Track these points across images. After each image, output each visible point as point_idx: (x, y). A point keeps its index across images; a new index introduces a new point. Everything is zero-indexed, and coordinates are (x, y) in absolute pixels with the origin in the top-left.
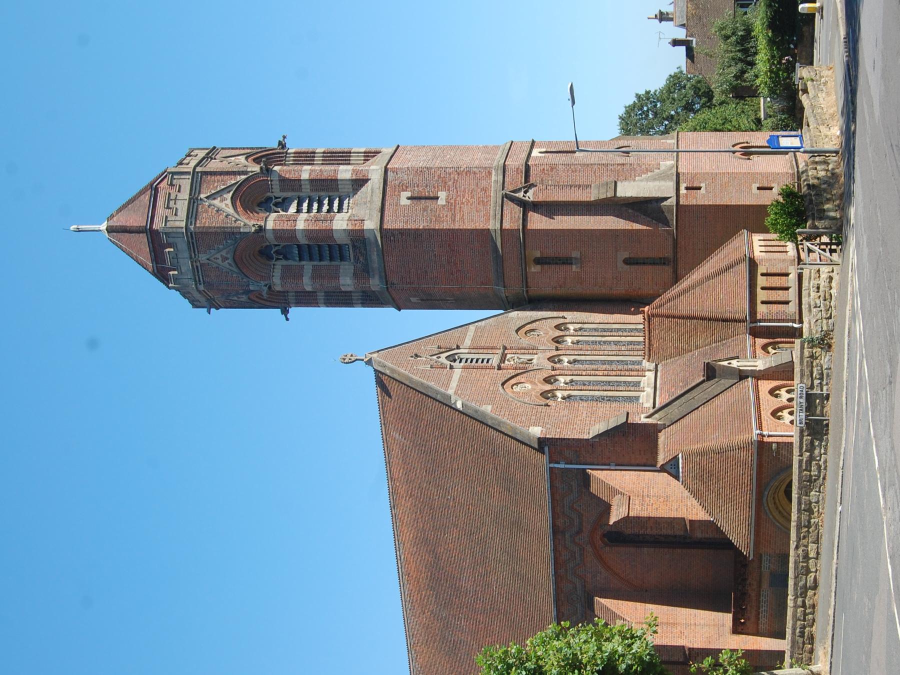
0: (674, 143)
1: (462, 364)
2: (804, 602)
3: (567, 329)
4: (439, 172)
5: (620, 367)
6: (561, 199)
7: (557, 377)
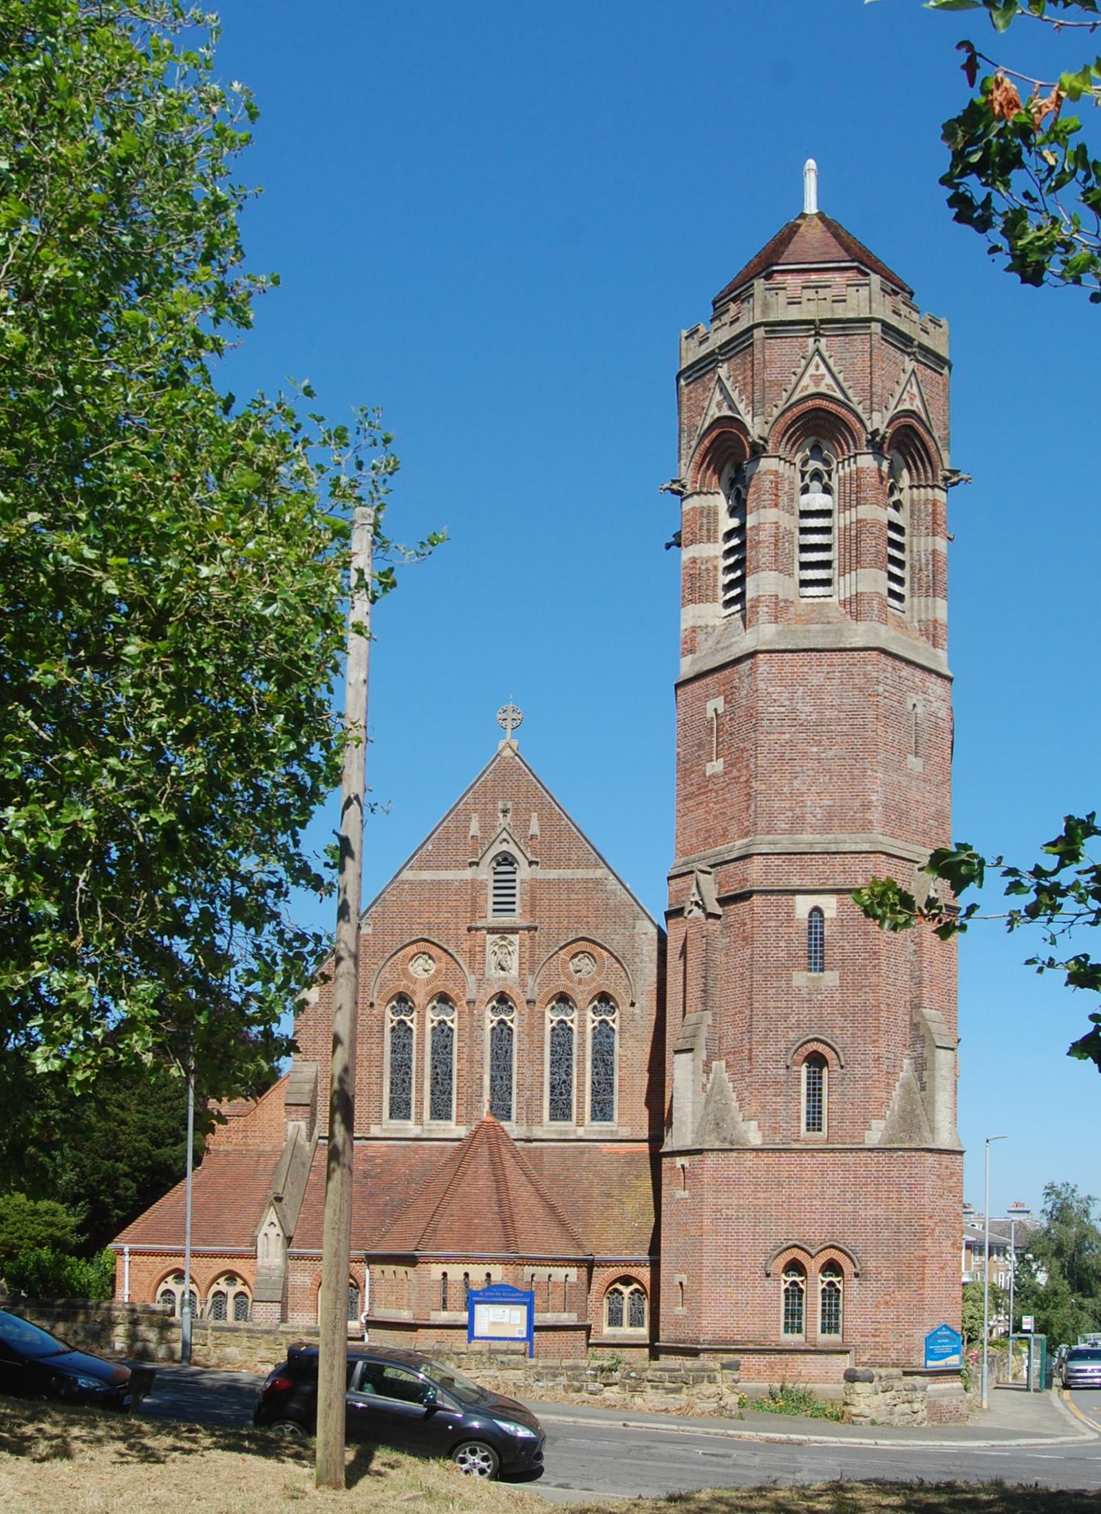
0: (863, 1143)
4: (749, 746)
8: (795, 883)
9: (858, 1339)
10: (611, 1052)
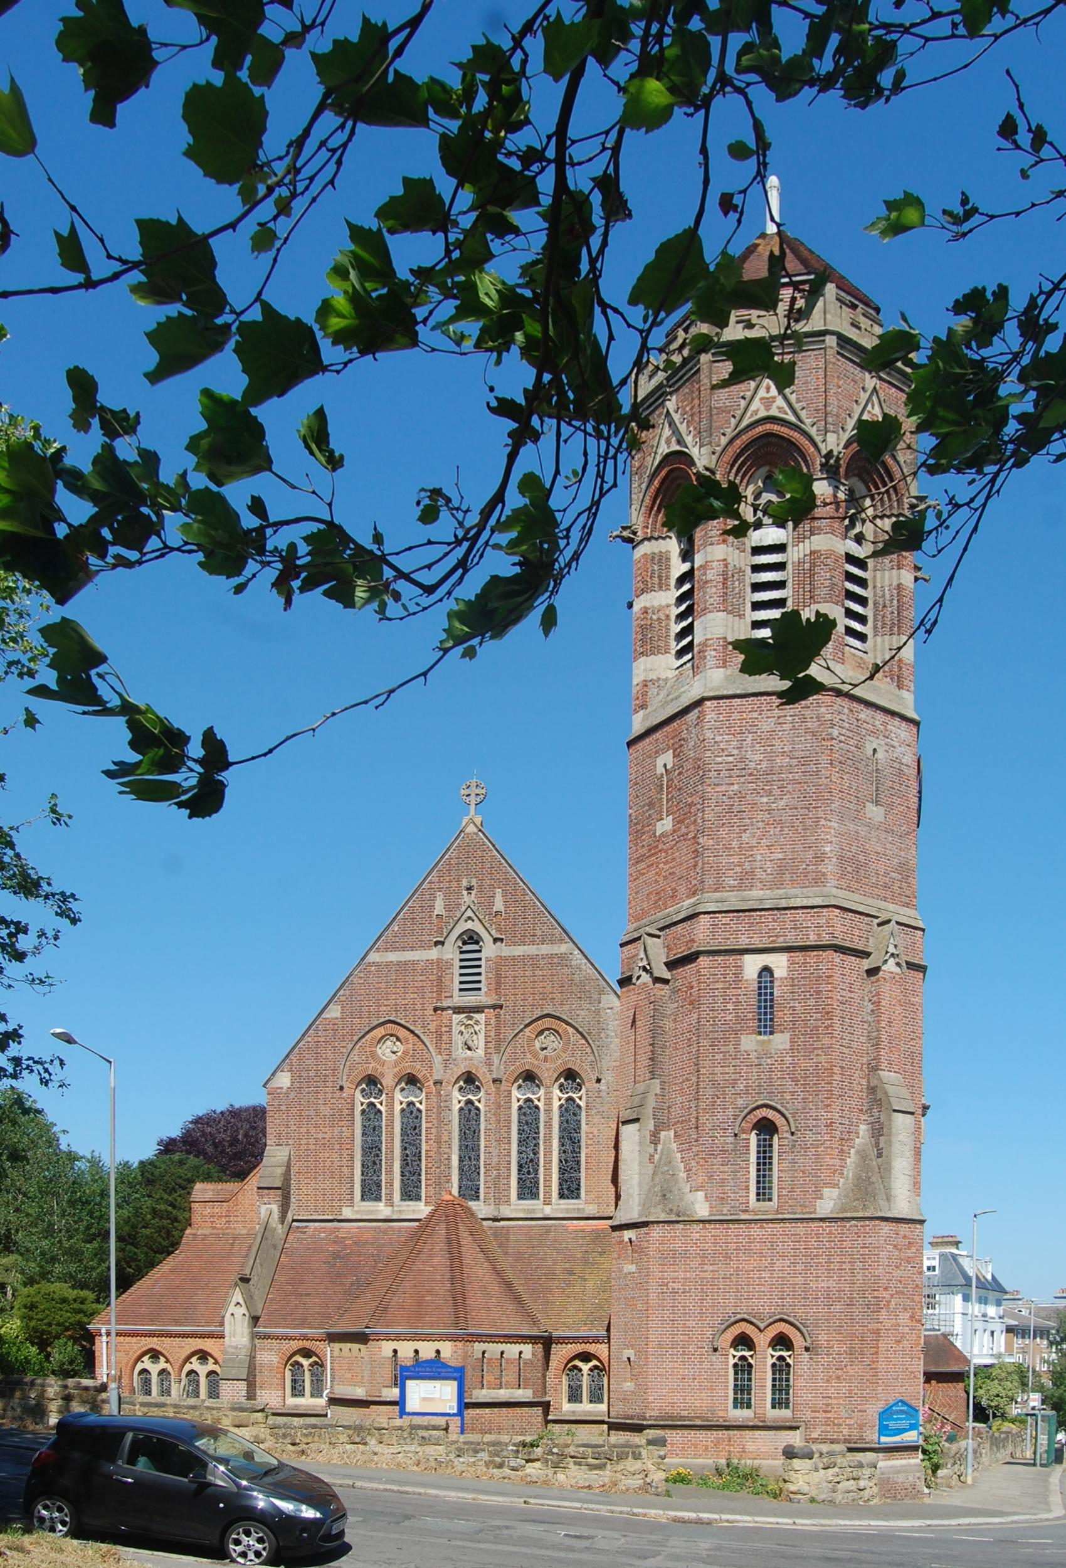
0: (814, 1213)
4: (697, 800)
8: (744, 941)
9: (808, 1415)
10: (578, 1129)
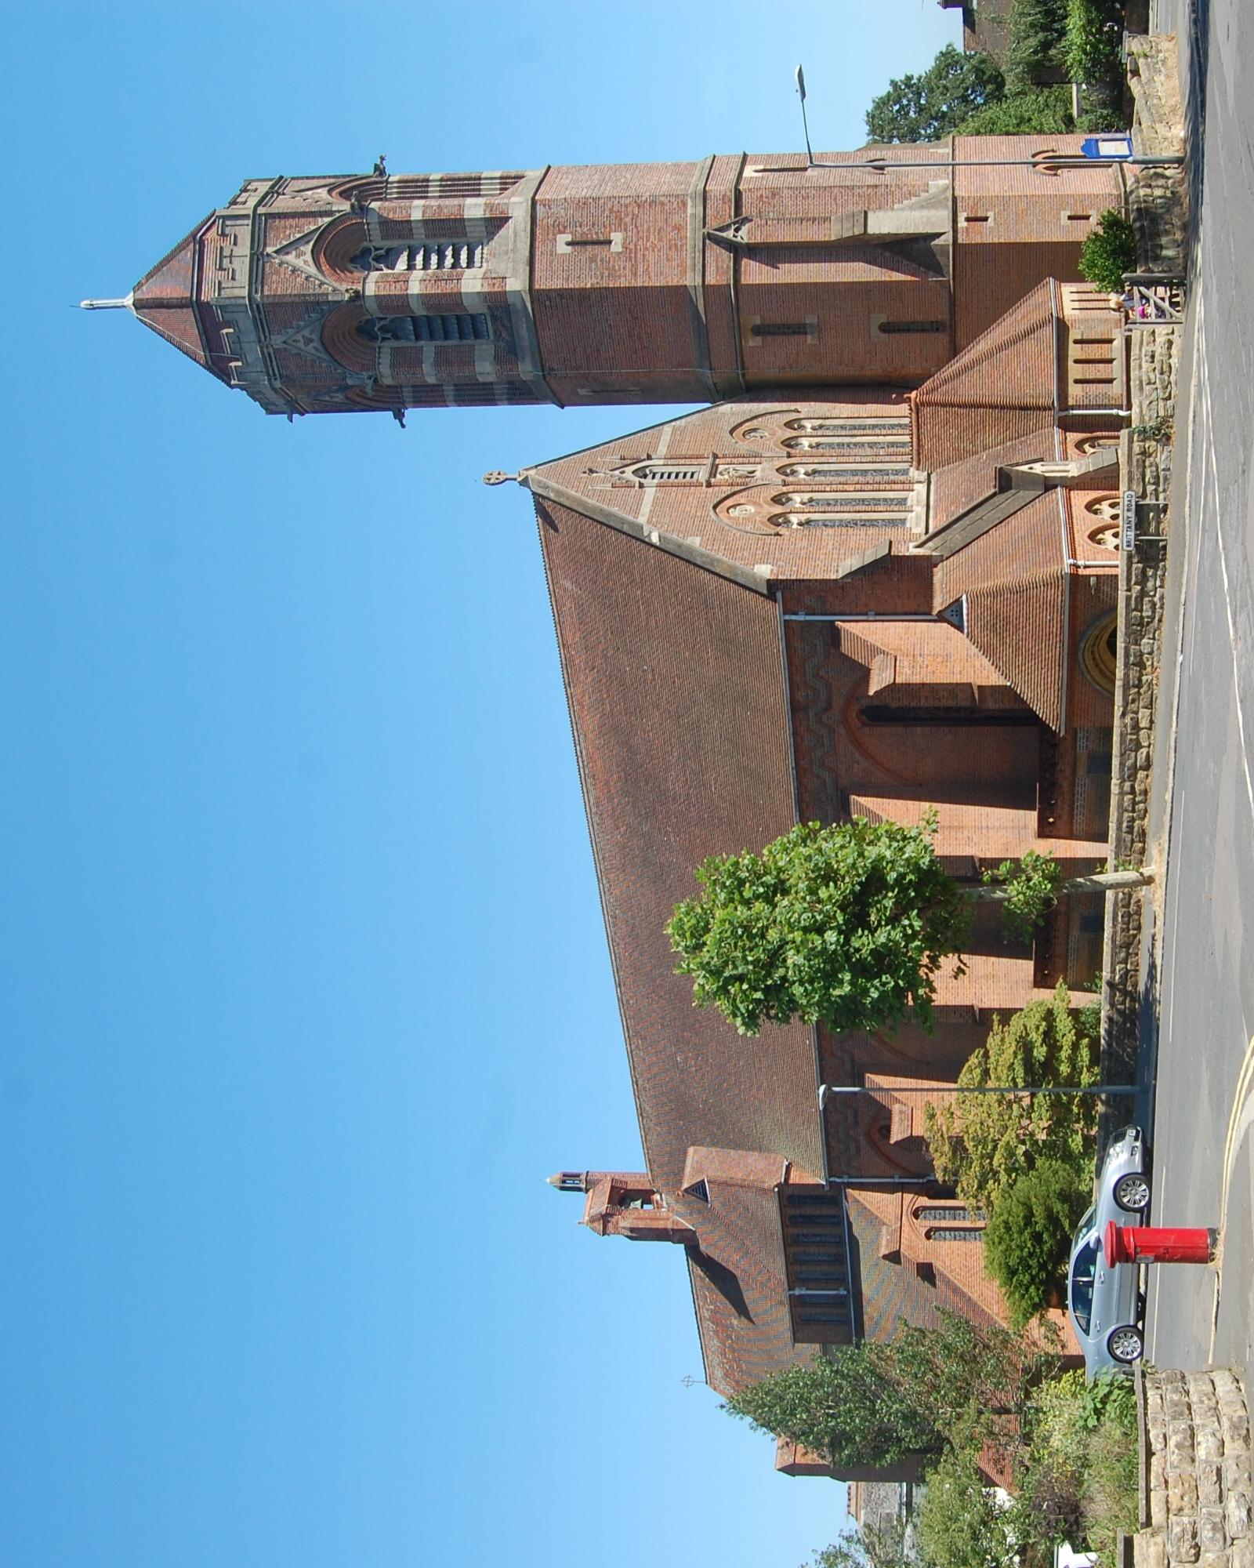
1: (656, 481)
2: (1133, 787)
3: (802, 427)
4: (610, 205)
5: (878, 479)
6: (787, 239)
7: (790, 495)
